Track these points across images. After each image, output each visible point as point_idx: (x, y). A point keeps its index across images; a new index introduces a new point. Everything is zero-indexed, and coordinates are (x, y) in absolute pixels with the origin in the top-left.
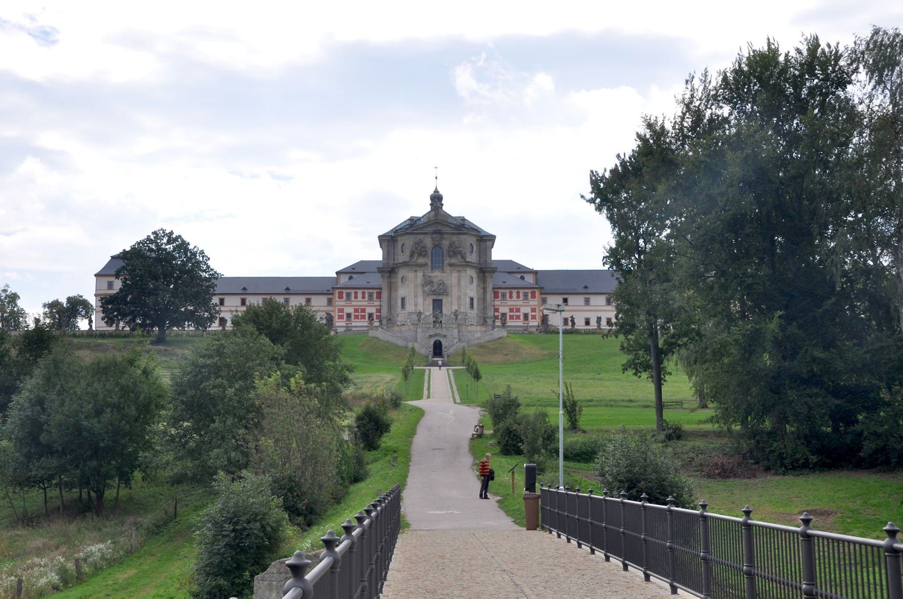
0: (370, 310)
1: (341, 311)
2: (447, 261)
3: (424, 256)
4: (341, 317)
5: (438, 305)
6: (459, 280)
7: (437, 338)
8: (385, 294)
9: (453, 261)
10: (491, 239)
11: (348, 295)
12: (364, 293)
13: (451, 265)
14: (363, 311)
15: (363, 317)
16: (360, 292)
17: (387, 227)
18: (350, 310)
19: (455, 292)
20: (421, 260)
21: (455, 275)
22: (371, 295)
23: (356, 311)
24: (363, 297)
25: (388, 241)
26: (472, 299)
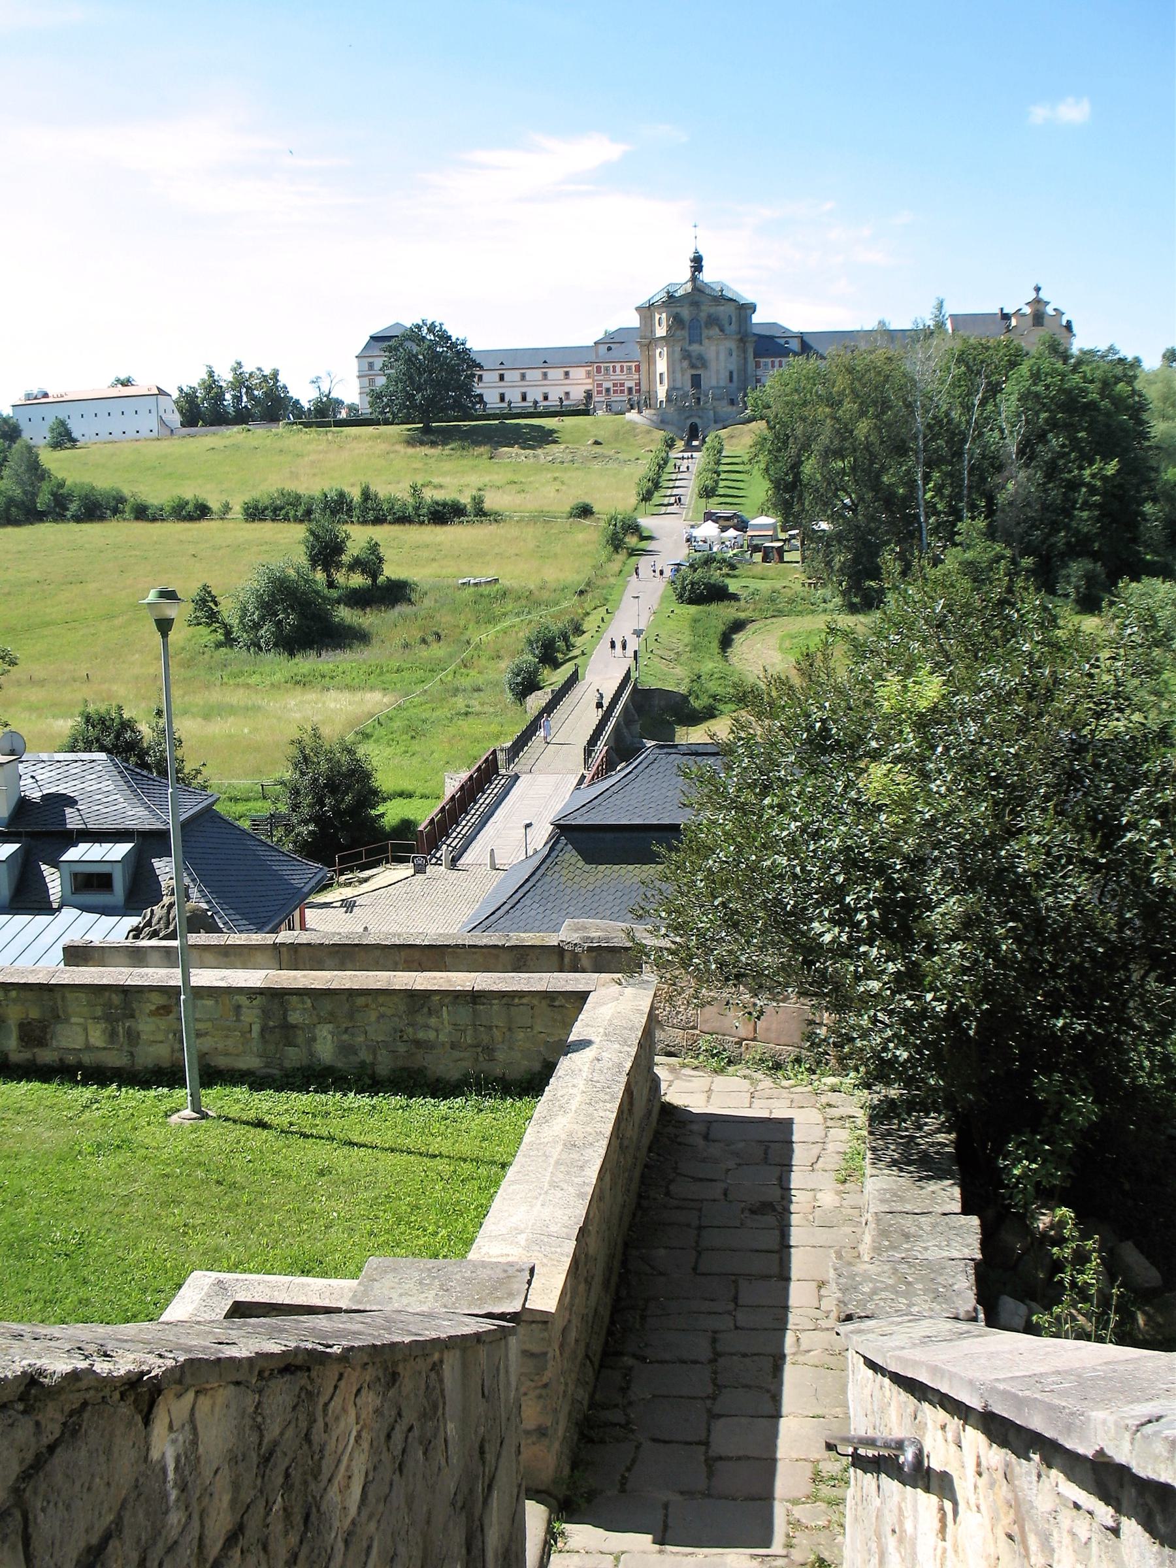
0: (628, 384)
1: (600, 385)
2: (705, 332)
3: (683, 329)
4: (599, 392)
5: (696, 381)
6: (718, 353)
7: (693, 420)
8: (644, 368)
9: (711, 333)
10: (752, 308)
11: (607, 369)
12: (622, 367)
13: (709, 338)
14: (622, 385)
15: (622, 392)
16: (618, 366)
17: (642, 300)
18: (606, 385)
19: (713, 365)
20: (679, 333)
21: (713, 348)
22: (629, 368)
23: (615, 385)
24: (622, 371)
25: (647, 311)
26: (731, 373)
